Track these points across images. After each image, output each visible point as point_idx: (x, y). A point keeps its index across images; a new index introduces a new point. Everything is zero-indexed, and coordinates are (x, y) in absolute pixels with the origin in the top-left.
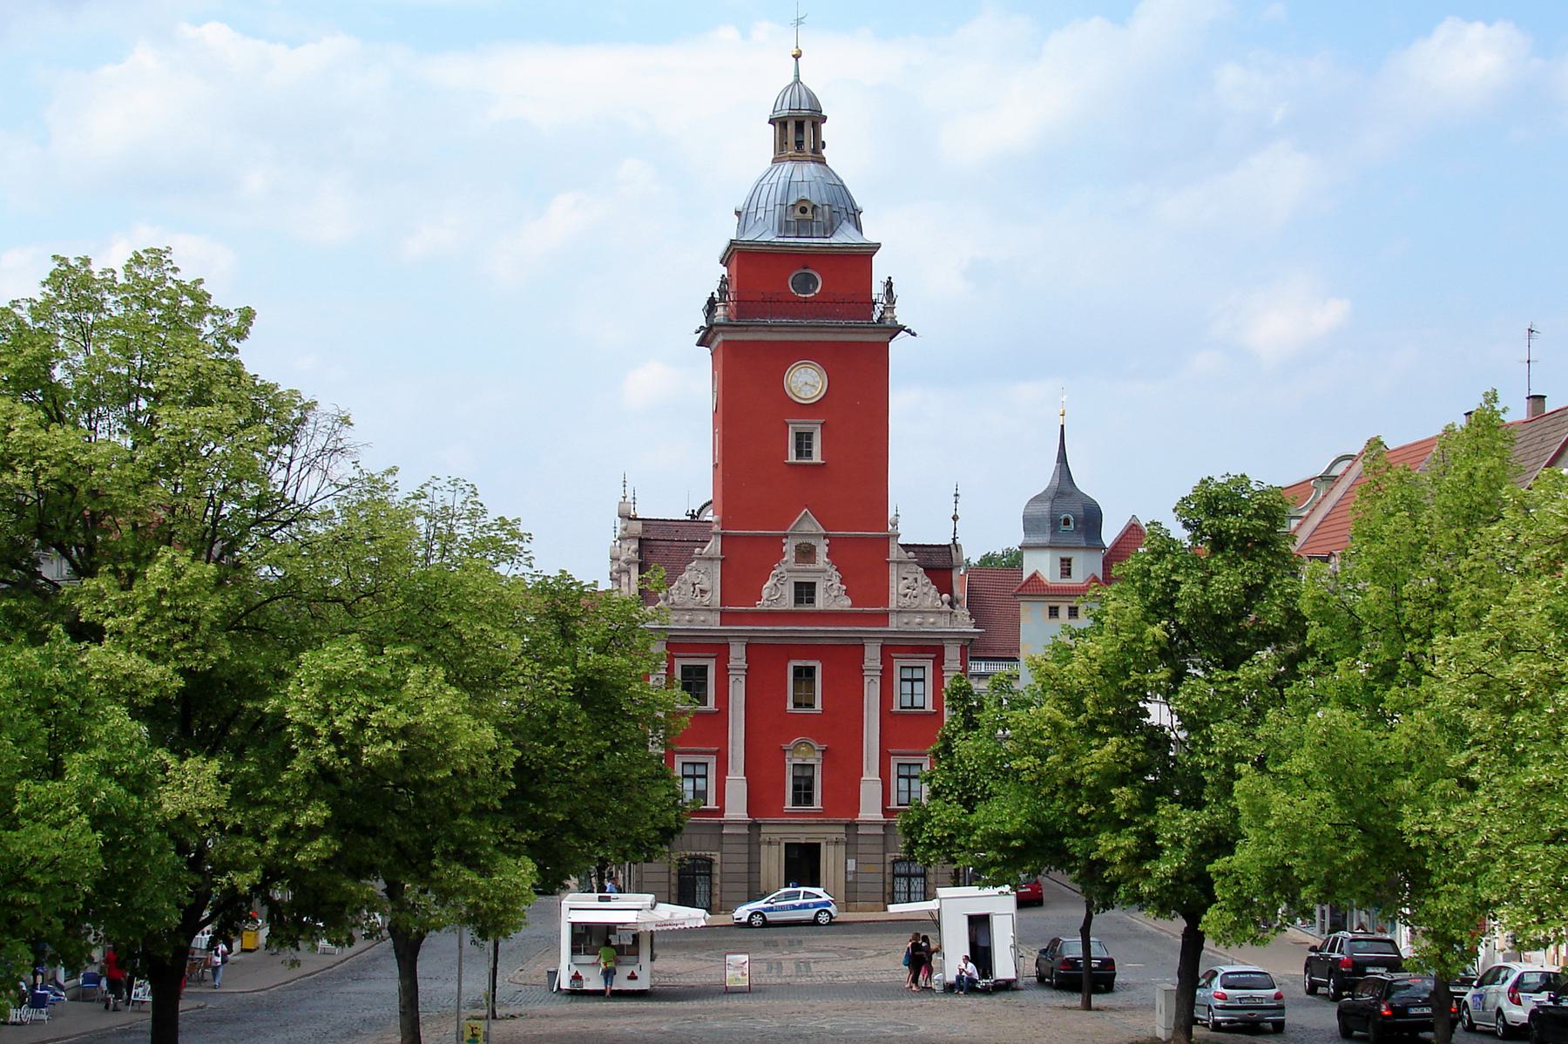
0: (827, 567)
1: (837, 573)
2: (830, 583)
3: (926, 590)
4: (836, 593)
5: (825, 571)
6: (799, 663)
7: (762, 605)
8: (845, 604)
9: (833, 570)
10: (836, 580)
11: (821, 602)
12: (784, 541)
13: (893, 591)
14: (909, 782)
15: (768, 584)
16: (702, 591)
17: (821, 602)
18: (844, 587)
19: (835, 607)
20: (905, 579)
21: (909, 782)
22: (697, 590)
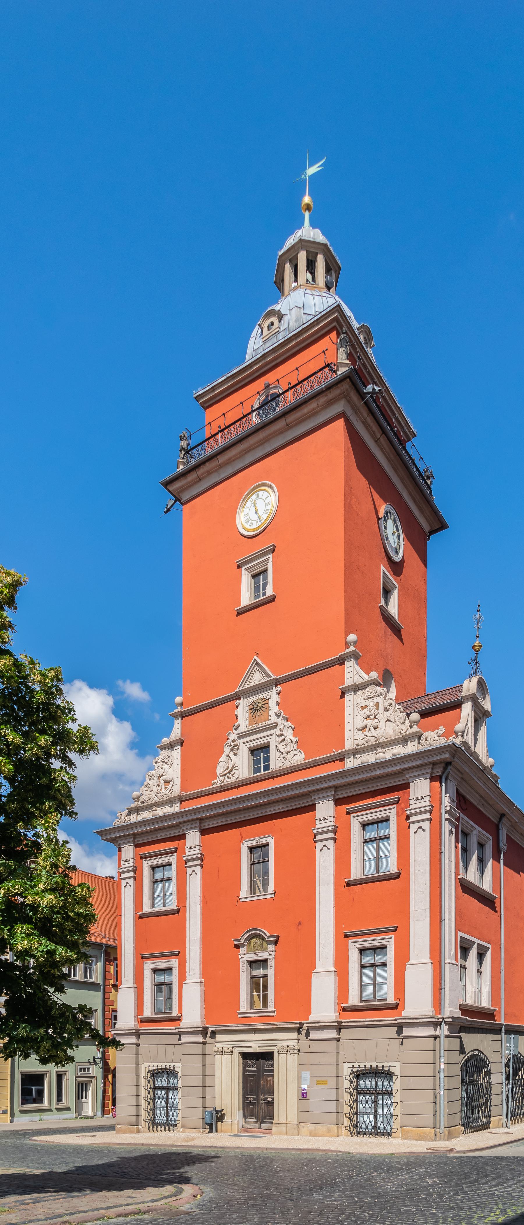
0: (279, 720)
1: (289, 724)
2: (283, 737)
3: (387, 714)
4: (289, 748)
5: (274, 726)
6: (253, 843)
7: (218, 782)
8: (299, 758)
9: (284, 722)
10: (289, 734)
11: (275, 764)
12: (237, 702)
13: (348, 727)
14: (375, 972)
15: (224, 757)
16: (167, 782)
17: (275, 764)
18: (295, 739)
19: (287, 764)
20: (364, 708)
21: (375, 972)
22: (162, 782)
